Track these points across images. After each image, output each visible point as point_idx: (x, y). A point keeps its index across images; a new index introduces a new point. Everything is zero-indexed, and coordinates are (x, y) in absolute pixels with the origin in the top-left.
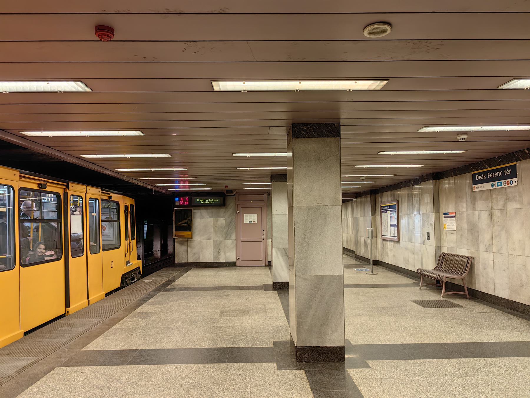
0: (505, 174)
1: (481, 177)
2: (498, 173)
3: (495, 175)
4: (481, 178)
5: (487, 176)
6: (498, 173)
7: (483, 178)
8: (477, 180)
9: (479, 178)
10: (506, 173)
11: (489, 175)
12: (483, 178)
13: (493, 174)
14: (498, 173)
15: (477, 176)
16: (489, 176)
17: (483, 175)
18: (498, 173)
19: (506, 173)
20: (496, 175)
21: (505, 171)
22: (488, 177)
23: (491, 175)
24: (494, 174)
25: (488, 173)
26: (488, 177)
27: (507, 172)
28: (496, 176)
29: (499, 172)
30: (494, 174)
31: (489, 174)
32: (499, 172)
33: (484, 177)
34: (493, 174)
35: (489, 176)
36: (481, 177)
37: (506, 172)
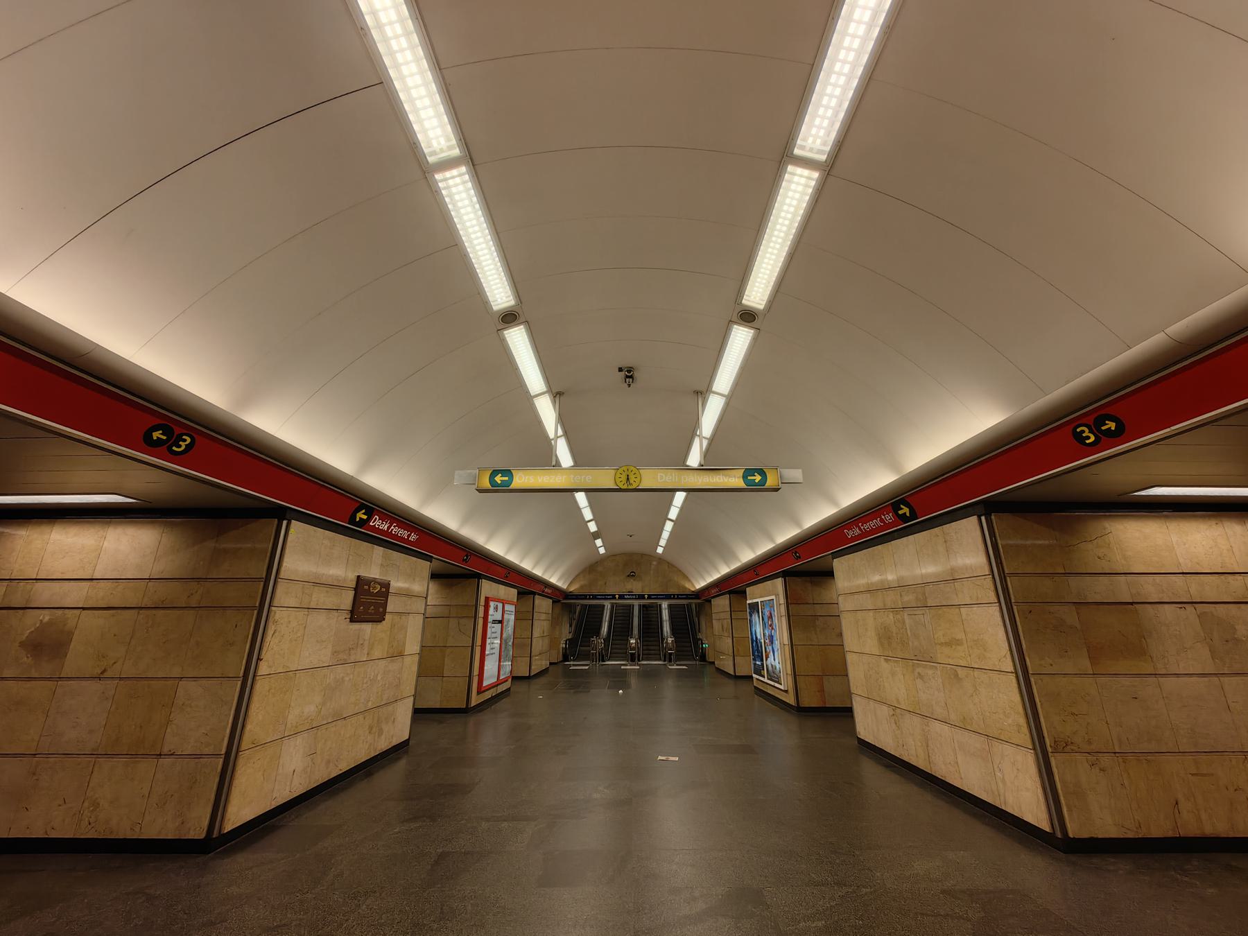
5: (389, 528)
8: (371, 524)
11: (392, 527)
16: (392, 529)
17: (386, 522)
33: (386, 527)
35: (392, 529)
36: (382, 523)
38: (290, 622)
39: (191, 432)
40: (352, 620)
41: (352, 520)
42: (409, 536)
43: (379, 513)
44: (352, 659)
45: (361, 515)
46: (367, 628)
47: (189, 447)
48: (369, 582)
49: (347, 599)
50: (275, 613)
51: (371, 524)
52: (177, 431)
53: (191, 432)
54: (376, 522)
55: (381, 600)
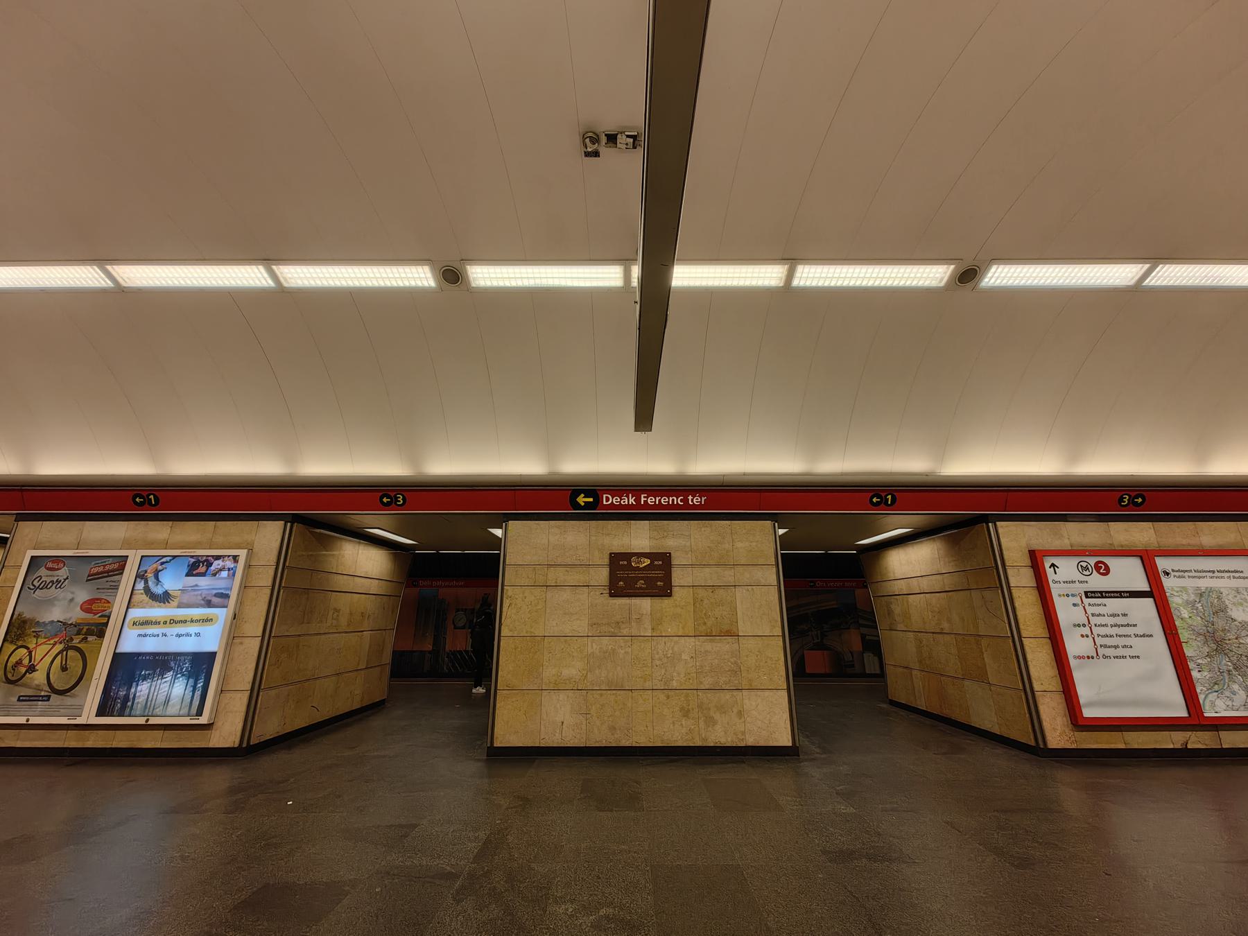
1: (621, 499)
2: (671, 499)
4: (620, 502)
5: (638, 500)
6: (671, 499)
7: (626, 503)
8: (605, 503)
9: (614, 501)
11: (643, 499)
12: (626, 503)
14: (673, 500)
15: (607, 497)
18: (673, 500)
21: (690, 498)
22: (642, 503)
23: (649, 501)
24: (660, 500)
25: (642, 496)
26: (642, 503)
31: (644, 497)
32: (675, 498)
34: (657, 499)
36: (621, 499)
37: (692, 501)
38: (525, 597)
39: (400, 492)
40: (611, 595)
41: (576, 506)
43: (607, 492)
44: (625, 632)
45: (581, 500)
46: (645, 605)
47: (404, 499)
48: (628, 556)
49: (603, 575)
50: (507, 590)
51: (605, 503)
52: (392, 494)
53: (400, 492)
54: (608, 500)
55: (660, 573)
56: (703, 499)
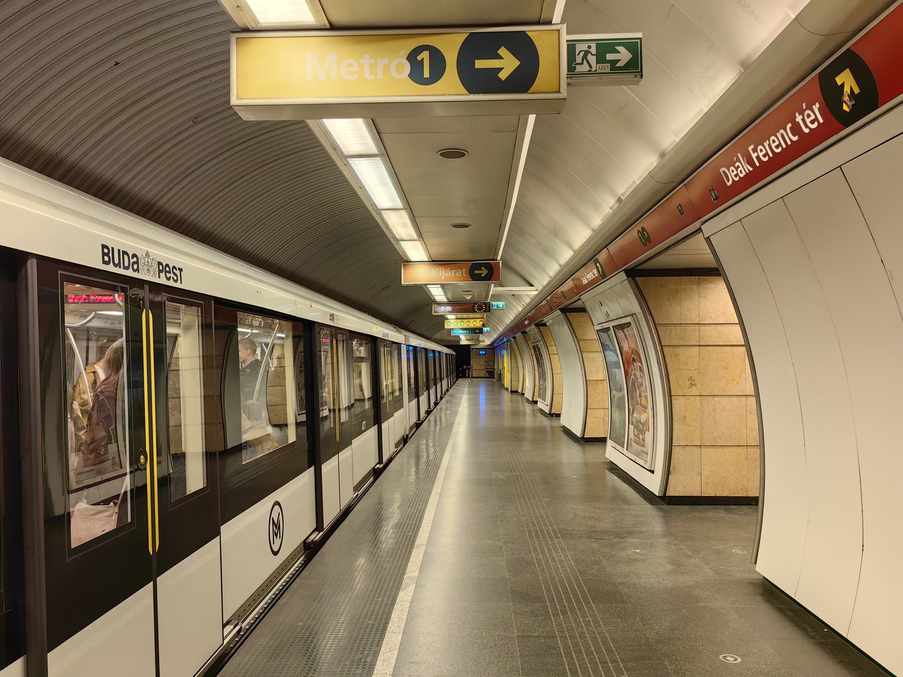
0: (806, 131)
3: (773, 146)
10: (807, 126)
11: (754, 155)
13: (766, 144)
14: (782, 136)
16: (758, 157)
18: (782, 136)
19: (807, 126)
20: (777, 147)
23: (761, 155)
24: (770, 146)
27: (808, 121)
28: (779, 150)
29: (782, 131)
30: (770, 146)
31: (755, 150)
32: (782, 131)
42: (796, 129)
56: (816, 107)
